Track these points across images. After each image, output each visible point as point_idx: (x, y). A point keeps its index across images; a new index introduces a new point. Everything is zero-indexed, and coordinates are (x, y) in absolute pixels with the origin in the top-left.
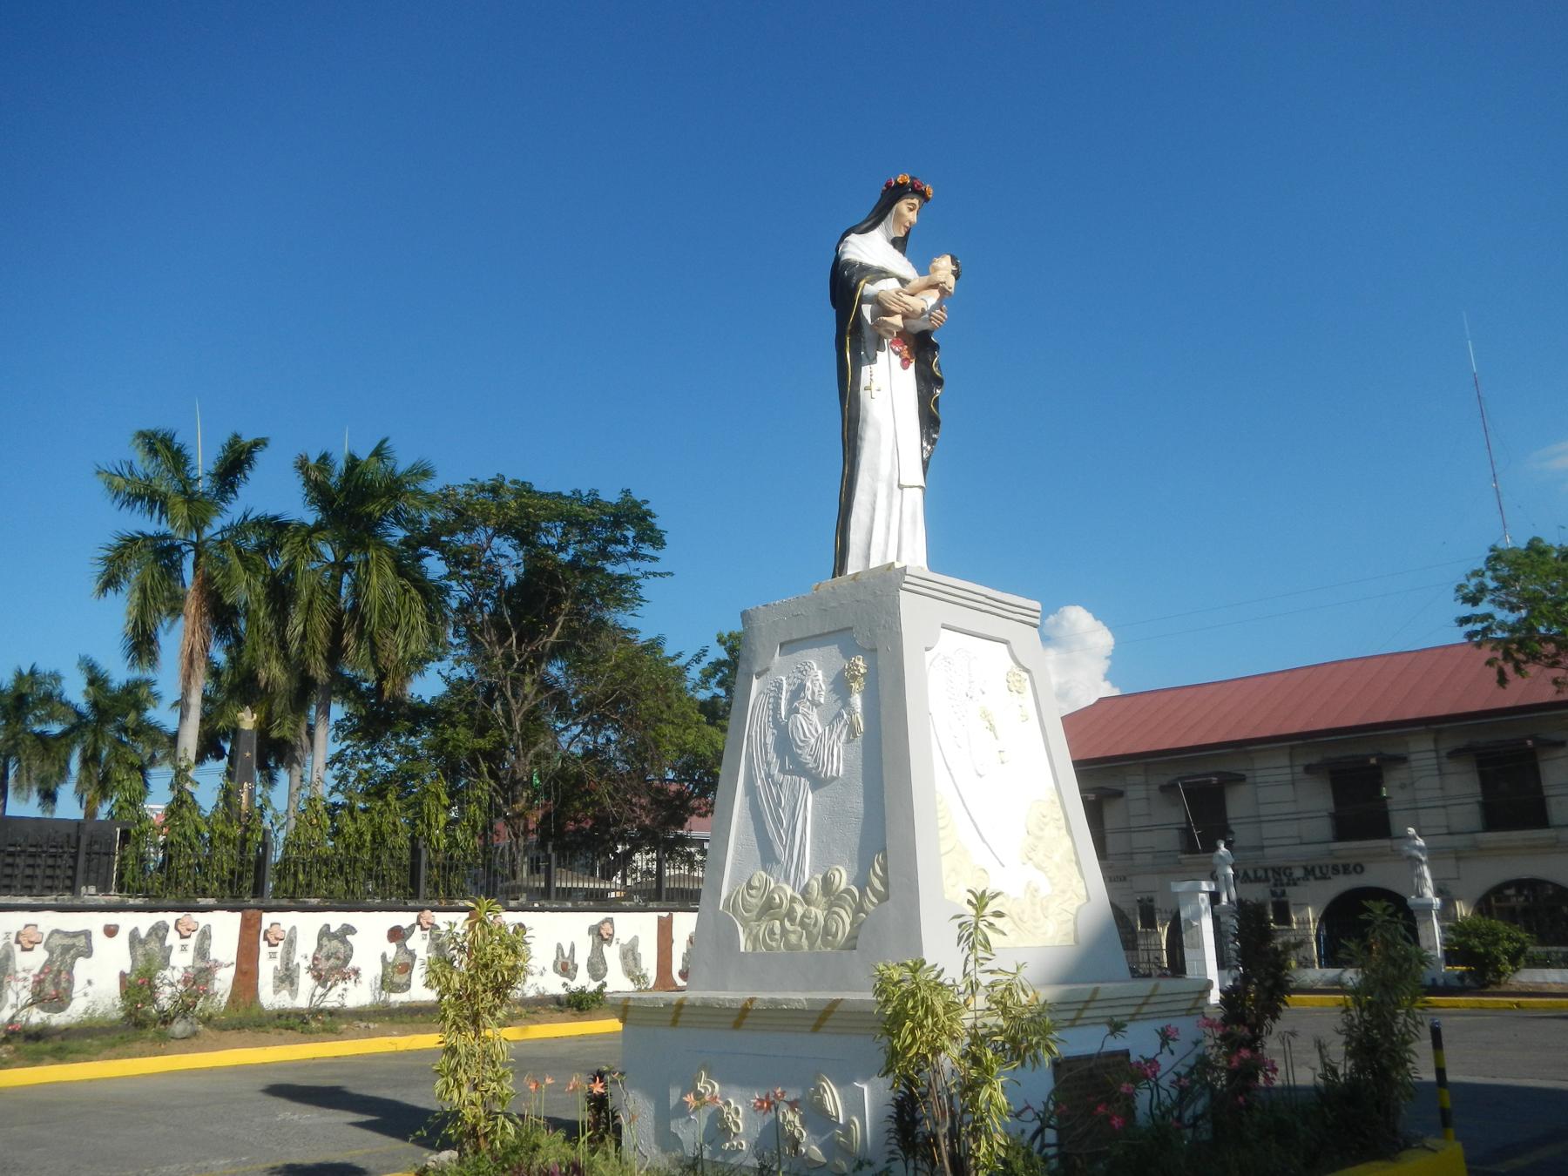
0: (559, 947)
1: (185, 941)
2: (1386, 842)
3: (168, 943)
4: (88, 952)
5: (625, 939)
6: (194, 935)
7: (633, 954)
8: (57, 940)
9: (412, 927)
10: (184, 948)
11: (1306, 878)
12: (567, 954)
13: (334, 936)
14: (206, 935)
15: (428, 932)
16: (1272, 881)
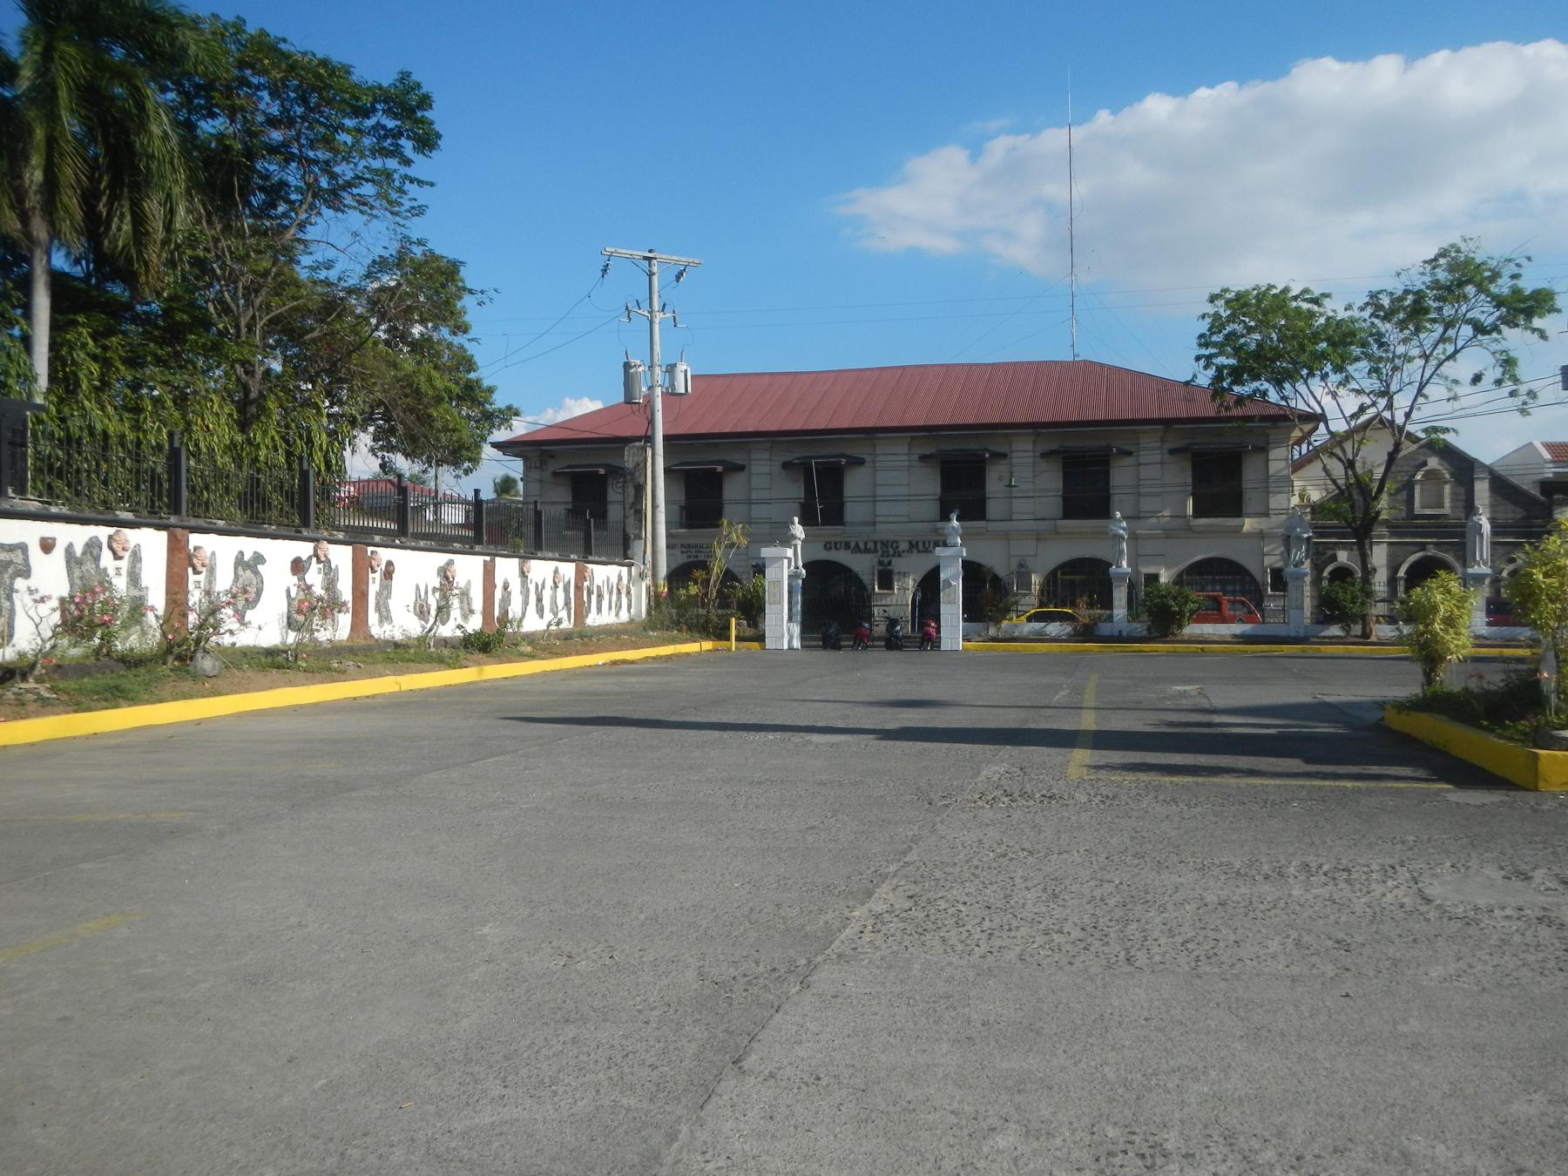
0: (418, 588)
1: (118, 563)
2: (982, 524)
3: (103, 564)
9: (310, 558)
11: (910, 551)
14: (136, 557)
15: (321, 566)
16: (880, 553)
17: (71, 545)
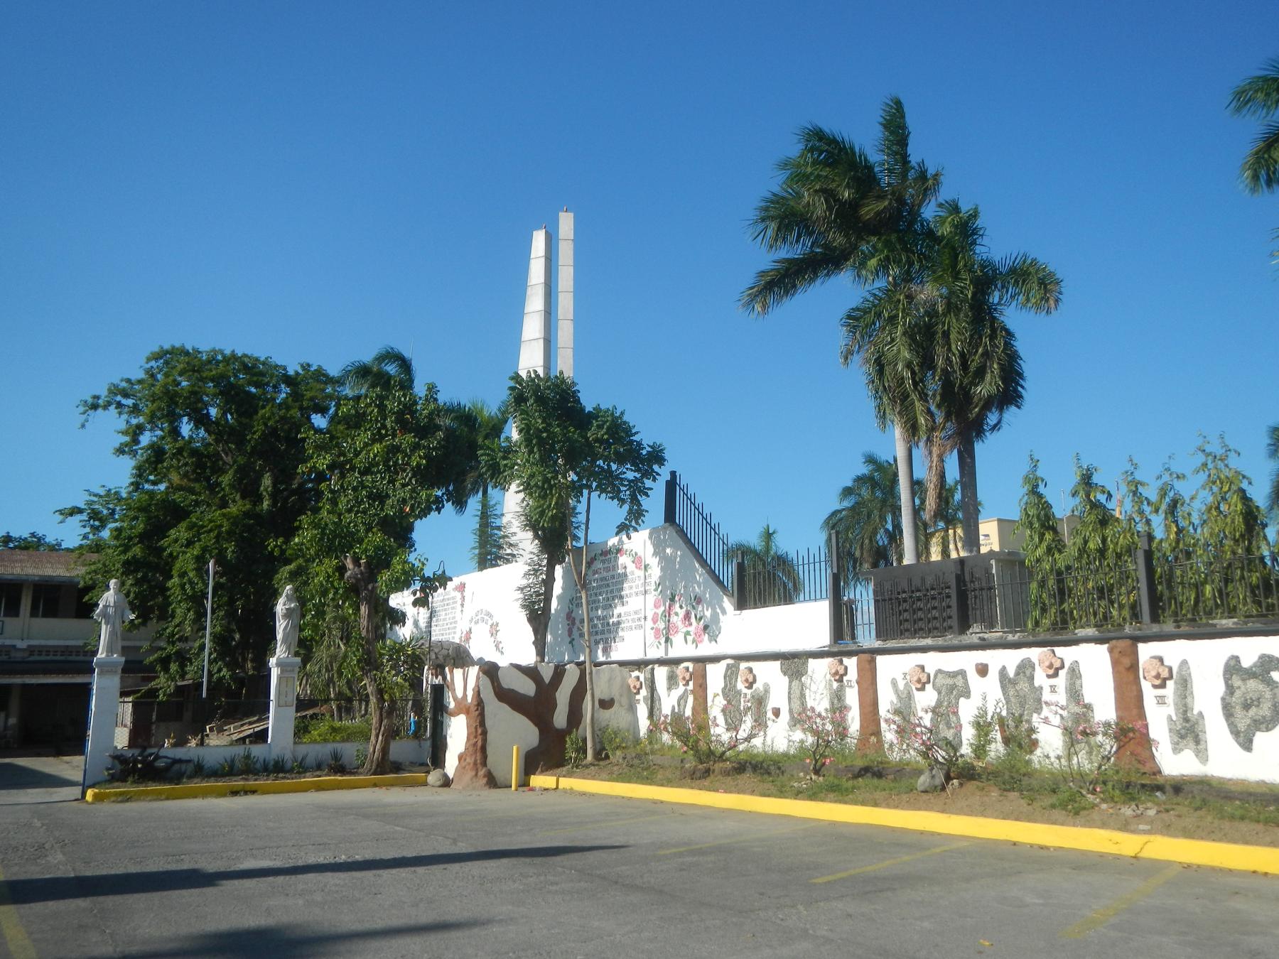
1: (1053, 681)
3: (1037, 684)
4: (966, 693)
6: (1062, 673)
8: (941, 681)
13: (1249, 674)
14: (1075, 673)
17: (1004, 668)
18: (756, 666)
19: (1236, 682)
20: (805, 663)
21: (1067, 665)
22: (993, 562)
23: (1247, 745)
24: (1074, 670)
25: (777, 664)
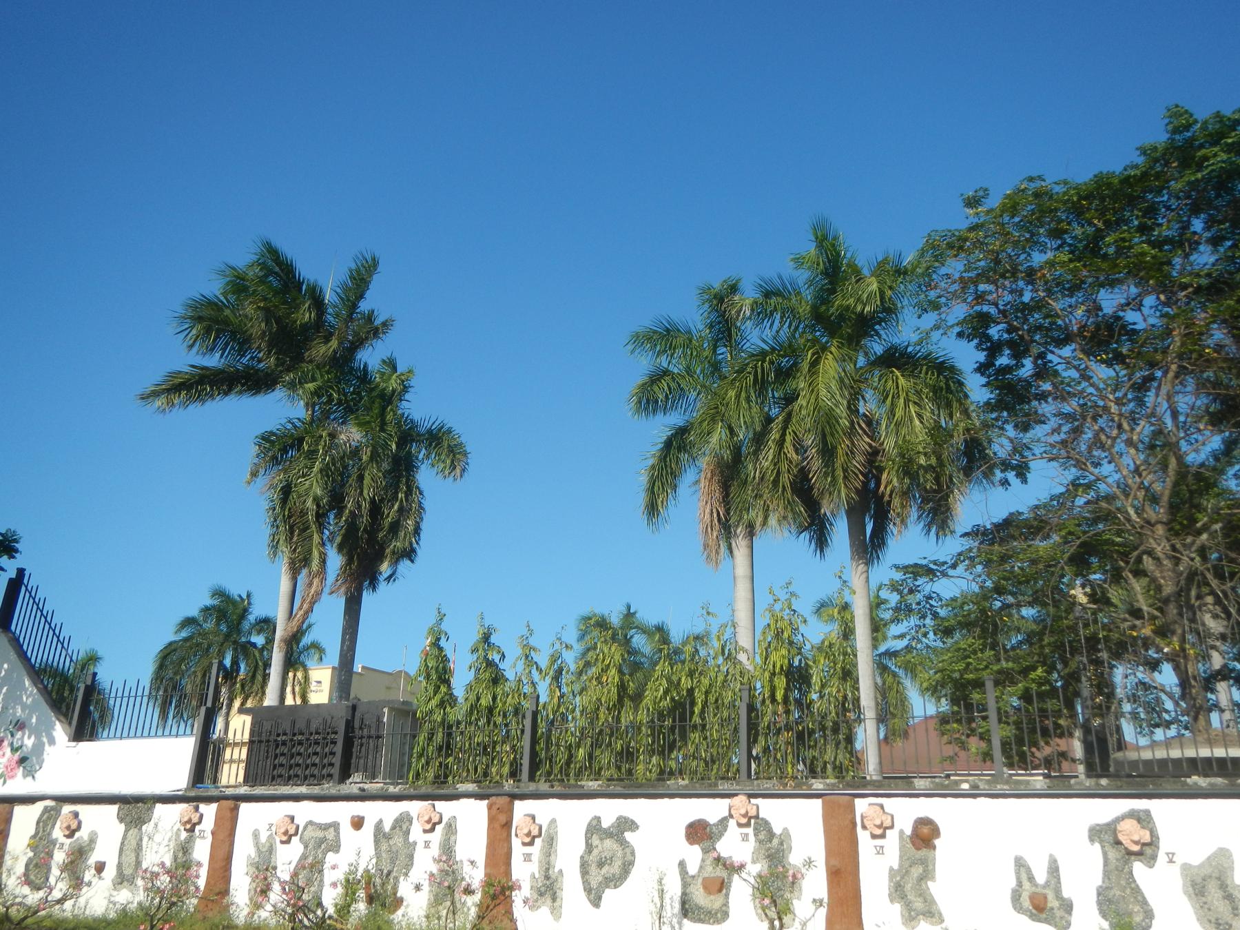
0: (1020, 864)
1: (428, 836)
3: (411, 839)
4: (336, 847)
5: (1197, 857)
6: (439, 828)
7: (1223, 886)
8: (311, 833)
9: (723, 822)
10: (427, 845)
12: (1041, 877)
13: (607, 834)
14: (451, 829)
15: (750, 831)
17: (381, 821)
18: (82, 809)
19: (595, 841)
20: (151, 809)
21: (445, 820)
22: (386, 710)
23: (596, 902)
24: (451, 825)
25: (113, 809)
